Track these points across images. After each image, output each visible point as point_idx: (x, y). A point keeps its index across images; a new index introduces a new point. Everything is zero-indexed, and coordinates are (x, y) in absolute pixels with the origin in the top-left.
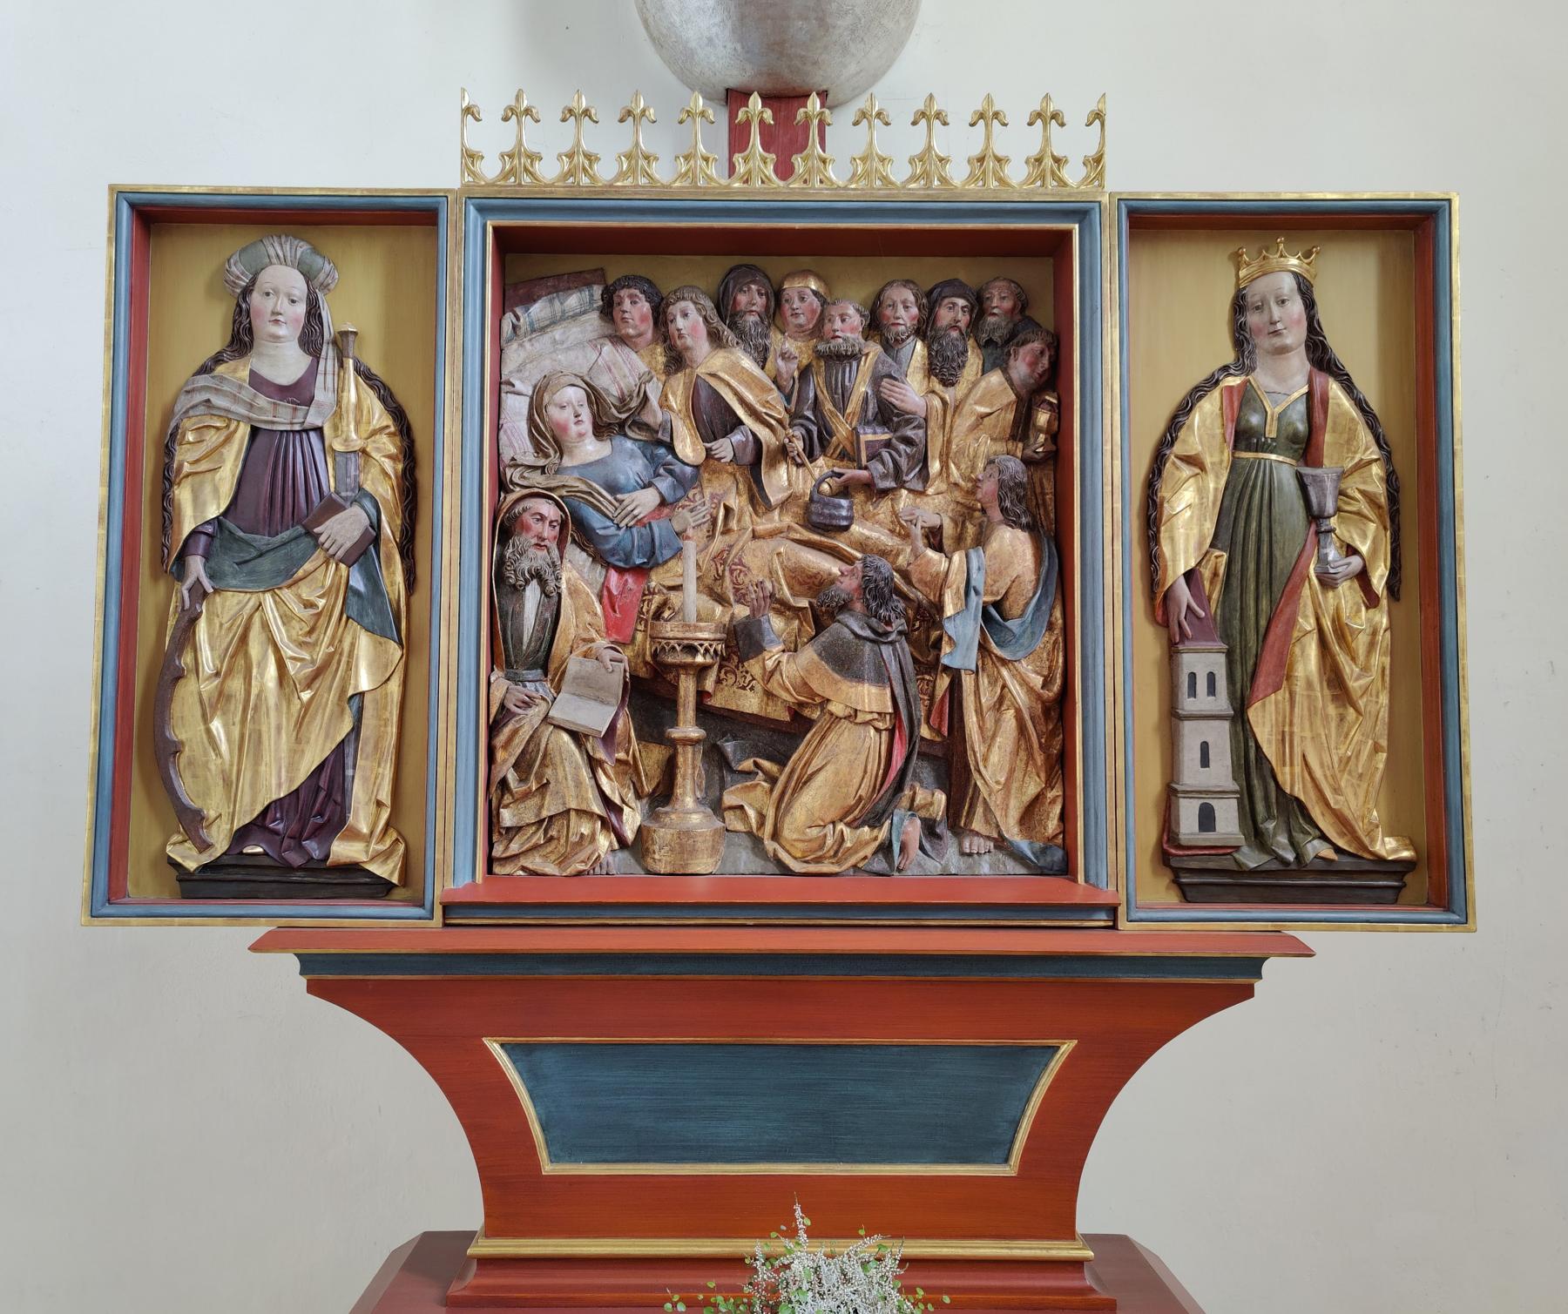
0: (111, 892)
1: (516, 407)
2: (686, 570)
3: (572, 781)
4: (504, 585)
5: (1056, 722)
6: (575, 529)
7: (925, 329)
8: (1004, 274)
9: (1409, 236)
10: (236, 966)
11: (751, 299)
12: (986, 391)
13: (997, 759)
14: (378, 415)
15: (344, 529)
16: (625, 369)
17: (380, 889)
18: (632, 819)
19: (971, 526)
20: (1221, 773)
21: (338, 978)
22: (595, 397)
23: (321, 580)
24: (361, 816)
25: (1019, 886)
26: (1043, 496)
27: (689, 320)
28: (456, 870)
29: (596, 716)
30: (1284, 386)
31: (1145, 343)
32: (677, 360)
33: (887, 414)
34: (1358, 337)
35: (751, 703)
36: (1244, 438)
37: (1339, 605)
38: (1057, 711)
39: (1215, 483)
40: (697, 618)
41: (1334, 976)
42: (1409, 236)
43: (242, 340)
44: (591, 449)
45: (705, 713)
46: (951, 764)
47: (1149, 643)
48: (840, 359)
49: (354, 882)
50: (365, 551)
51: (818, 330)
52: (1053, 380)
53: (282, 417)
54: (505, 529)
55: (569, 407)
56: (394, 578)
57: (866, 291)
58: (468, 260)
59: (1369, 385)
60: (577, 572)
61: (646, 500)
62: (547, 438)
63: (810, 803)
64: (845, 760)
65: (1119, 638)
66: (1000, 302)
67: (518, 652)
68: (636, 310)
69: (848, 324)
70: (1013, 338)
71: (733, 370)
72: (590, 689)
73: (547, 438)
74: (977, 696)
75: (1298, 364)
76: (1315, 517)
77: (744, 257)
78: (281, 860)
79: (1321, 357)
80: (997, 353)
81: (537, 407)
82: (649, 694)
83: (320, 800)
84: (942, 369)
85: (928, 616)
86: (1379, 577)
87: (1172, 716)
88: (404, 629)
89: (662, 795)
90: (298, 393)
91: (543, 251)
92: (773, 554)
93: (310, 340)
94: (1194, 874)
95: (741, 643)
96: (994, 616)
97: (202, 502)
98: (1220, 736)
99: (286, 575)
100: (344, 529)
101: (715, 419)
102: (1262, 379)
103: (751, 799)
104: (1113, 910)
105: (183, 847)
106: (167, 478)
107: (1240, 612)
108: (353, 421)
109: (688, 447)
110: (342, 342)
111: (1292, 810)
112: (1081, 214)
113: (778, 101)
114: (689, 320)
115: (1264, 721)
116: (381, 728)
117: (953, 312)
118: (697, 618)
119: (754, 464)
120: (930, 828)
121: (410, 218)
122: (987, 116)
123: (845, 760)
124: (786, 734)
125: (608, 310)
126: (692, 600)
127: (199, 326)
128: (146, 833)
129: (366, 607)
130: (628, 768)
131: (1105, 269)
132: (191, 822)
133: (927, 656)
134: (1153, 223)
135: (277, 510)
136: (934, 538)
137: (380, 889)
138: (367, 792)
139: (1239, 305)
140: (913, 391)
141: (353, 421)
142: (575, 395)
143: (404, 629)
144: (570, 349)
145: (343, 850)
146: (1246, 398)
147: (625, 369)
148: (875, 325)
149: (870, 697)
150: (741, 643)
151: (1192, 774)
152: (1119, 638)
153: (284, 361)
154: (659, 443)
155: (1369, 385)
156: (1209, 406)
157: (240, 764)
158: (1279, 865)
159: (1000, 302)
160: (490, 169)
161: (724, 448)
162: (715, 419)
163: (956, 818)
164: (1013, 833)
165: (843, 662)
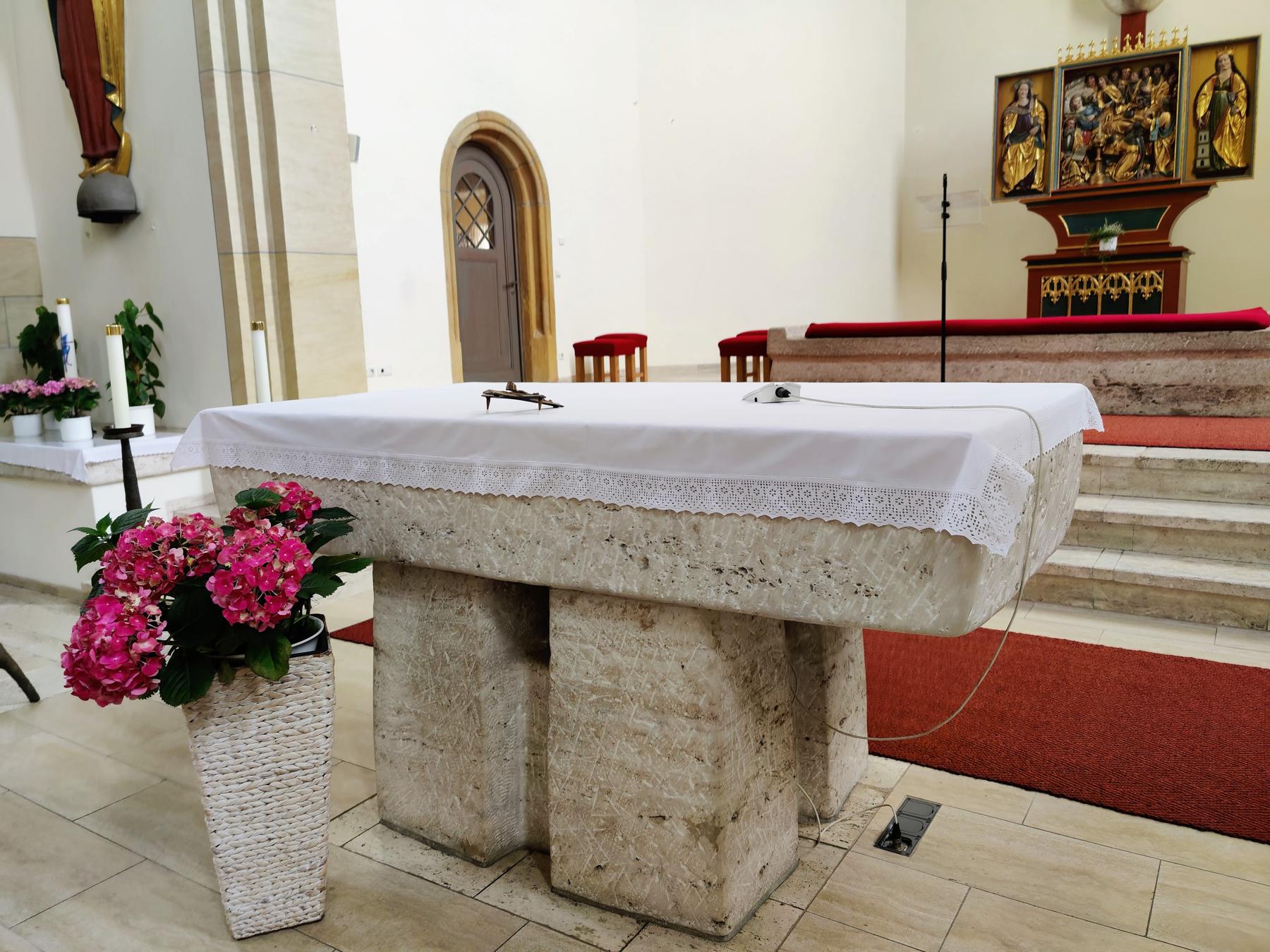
0: (994, 198)
1: (1068, 103)
2: (1099, 130)
3: (1076, 169)
4: (1064, 137)
6: (1078, 124)
7: (1152, 74)
9: (1252, 43)
10: (1016, 207)
11: (1115, 75)
12: (1164, 85)
13: (1160, 155)
14: (1041, 108)
15: (1035, 130)
16: (1089, 92)
17: (1040, 193)
18: (1087, 176)
19: (1158, 113)
20: (1207, 153)
21: (1032, 206)
22: (1083, 98)
23: (1031, 140)
24: (1037, 181)
25: (1163, 179)
26: (1171, 105)
27: (1102, 81)
28: (1054, 186)
29: (1081, 158)
30: (1225, 75)
31: (1193, 74)
32: (1100, 88)
33: (1142, 93)
34: (1242, 65)
35: (1111, 152)
36: (1216, 88)
38: (1172, 146)
39: (1209, 98)
40: (1101, 137)
41: (1224, 189)
43: (1016, 98)
44: (1082, 109)
45: (1102, 155)
46: (1151, 159)
47: (1193, 131)
48: (1134, 83)
49: (1035, 192)
50: (1038, 134)
51: (1129, 78)
52: (1173, 85)
53: (1024, 112)
54: (1065, 126)
55: (1078, 100)
56: (1044, 138)
57: (1139, 69)
58: (1059, 79)
59: (1244, 73)
60: (1078, 133)
61: (1092, 117)
62: (1073, 108)
63: (1122, 169)
64: (1129, 161)
65: (1185, 129)
66: (1167, 67)
67: (1067, 148)
68: (1092, 80)
69: (1135, 76)
70: (1170, 74)
71: (1111, 90)
72: (1079, 153)
73: (1073, 108)
74: (1157, 145)
75: (1229, 72)
76: (1231, 103)
78: (1023, 189)
79: (1235, 70)
80: (1166, 79)
81: (1071, 102)
82: (1091, 153)
83: (1030, 179)
84: (1155, 82)
85: (1147, 132)
86: (1243, 112)
87: (1197, 145)
88: (1046, 147)
89: (1093, 172)
90: (1027, 107)
91: (1074, 73)
92: (1117, 125)
93: (1029, 97)
95: (1109, 141)
96: (1162, 130)
97: (1009, 130)
98: (1207, 148)
99: (1024, 140)
100: (1035, 130)
101: (1106, 99)
102: (1221, 76)
103: (1111, 171)
104: (1179, 181)
105: (1003, 189)
106: (1002, 126)
107: (1213, 124)
108: (1037, 110)
109: (1101, 105)
110: (1035, 97)
111: (1221, 160)
112: (1182, 50)
114: (1102, 81)
115: (1216, 144)
116: (1040, 165)
117: (1158, 71)
118: (1101, 137)
119: (1115, 106)
120: (1146, 172)
121: (1050, 71)
122: (1163, 33)
123: (1129, 161)
124: (1117, 158)
125: (1086, 81)
126: (1100, 134)
127: (1010, 98)
128: (999, 188)
129: (1039, 144)
130: (1087, 168)
131: (1185, 61)
132: (1007, 185)
133: (1147, 140)
134: (1196, 49)
136: (1151, 117)
137: (1040, 193)
139: (1217, 61)
140: (1148, 88)
142: (1079, 99)
143: (1046, 147)
144: (1079, 90)
145: (1033, 187)
146: (1218, 80)
147: (1089, 92)
148: (1141, 75)
149: (1134, 148)
150: (1109, 141)
151: (1200, 155)
152: (1185, 129)
153: (1024, 101)
154: (1095, 105)
155: (1244, 73)
156: (1210, 82)
157: (1015, 175)
158: (1217, 170)
159: (1167, 67)
160: (1063, 60)
161: (1108, 105)
162: (1106, 99)
163: (1152, 169)
164: (1162, 169)
165: (1129, 142)
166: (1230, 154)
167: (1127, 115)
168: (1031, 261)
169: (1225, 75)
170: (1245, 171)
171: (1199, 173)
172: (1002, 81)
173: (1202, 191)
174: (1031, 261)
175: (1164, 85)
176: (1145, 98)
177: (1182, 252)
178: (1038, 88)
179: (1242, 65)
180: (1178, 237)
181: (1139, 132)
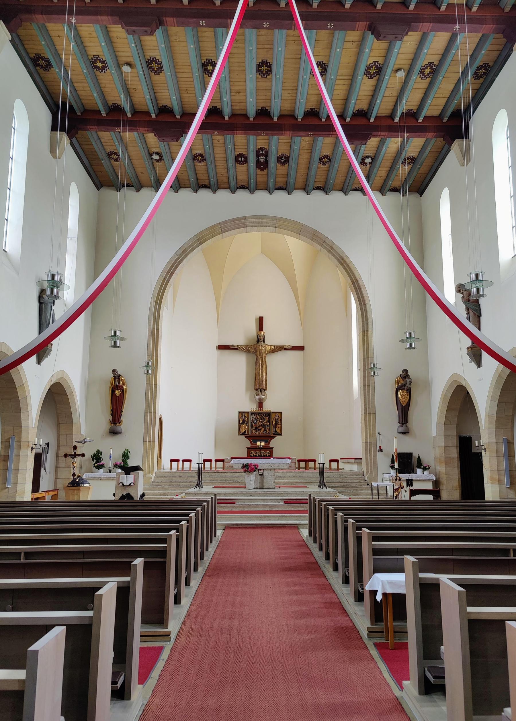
3: (254, 431)
5: (269, 429)
8: (268, 414)
9: (281, 413)
10: (243, 437)
12: (267, 418)
21: (246, 437)
26: (269, 421)
30: (277, 418)
31: (272, 417)
34: (280, 416)
37: (279, 425)
40: (257, 426)
42: (281, 413)
46: (266, 430)
58: (250, 414)
64: (262, 430)
67: (252, 427)
71: (259, 417)
77: (259, 414)
78: (244, 434)
82: (256, 428)
91: (252, 413)
94: (274, 434)
105: (241, 433)
107: (275, 426)
108: (246, 419)
113: (260, 405)
118: (257, 426)
123: (262, 430)
124: (260, 430)
129: (246, 425)
135: (244, 422)
138: (247, 431)
141: (246, 419)
144: (253, 416)
157: (243, 431)
158: (277, 434)
166: (279, 432)
167: (262, 422)
168: (248, 448)
169: (277, 418)
170: (281, 434)
171: (274, 434)
172: (239, 412)
173: (275, 437)
174: (248, 448)
175: (267, 418)
176: (264, 420)
177: (272, 448)
178: (246, 415)
179: (280, 416)
180: (271, 446)
181: (263, 425)
